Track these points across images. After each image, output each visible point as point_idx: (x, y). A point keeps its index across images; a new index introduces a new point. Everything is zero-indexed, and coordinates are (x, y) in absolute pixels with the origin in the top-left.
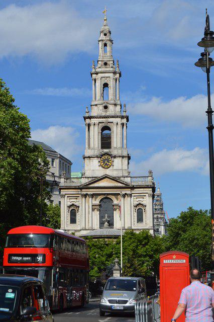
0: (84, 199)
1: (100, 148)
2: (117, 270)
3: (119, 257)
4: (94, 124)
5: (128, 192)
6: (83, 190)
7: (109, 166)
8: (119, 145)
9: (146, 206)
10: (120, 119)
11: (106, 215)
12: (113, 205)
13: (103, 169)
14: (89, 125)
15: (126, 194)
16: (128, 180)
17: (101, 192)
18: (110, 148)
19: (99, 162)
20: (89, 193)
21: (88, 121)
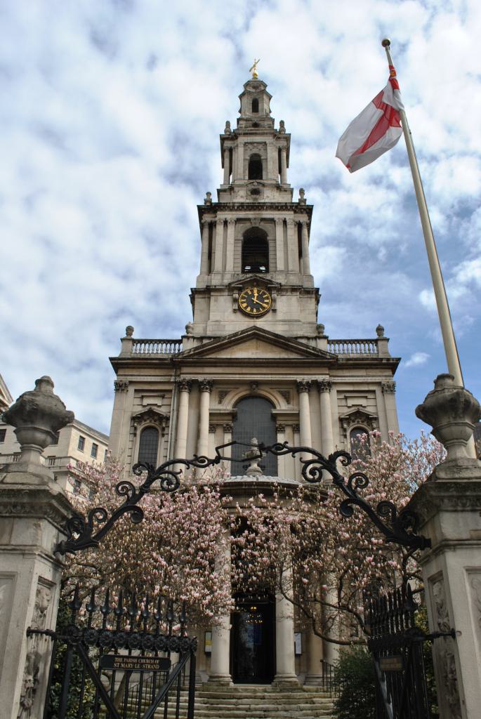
0: (185, 397)
4: (226, 223)
5: (320, 378)
6: (185, 370)
9: (376, 419)
12: (274, 417)
13: (247, 319)
14: (212, 226)
16: (322, 345)
17: (237, 377)
19: (235, 300)
20: (200, 378)
21: (208, 218)
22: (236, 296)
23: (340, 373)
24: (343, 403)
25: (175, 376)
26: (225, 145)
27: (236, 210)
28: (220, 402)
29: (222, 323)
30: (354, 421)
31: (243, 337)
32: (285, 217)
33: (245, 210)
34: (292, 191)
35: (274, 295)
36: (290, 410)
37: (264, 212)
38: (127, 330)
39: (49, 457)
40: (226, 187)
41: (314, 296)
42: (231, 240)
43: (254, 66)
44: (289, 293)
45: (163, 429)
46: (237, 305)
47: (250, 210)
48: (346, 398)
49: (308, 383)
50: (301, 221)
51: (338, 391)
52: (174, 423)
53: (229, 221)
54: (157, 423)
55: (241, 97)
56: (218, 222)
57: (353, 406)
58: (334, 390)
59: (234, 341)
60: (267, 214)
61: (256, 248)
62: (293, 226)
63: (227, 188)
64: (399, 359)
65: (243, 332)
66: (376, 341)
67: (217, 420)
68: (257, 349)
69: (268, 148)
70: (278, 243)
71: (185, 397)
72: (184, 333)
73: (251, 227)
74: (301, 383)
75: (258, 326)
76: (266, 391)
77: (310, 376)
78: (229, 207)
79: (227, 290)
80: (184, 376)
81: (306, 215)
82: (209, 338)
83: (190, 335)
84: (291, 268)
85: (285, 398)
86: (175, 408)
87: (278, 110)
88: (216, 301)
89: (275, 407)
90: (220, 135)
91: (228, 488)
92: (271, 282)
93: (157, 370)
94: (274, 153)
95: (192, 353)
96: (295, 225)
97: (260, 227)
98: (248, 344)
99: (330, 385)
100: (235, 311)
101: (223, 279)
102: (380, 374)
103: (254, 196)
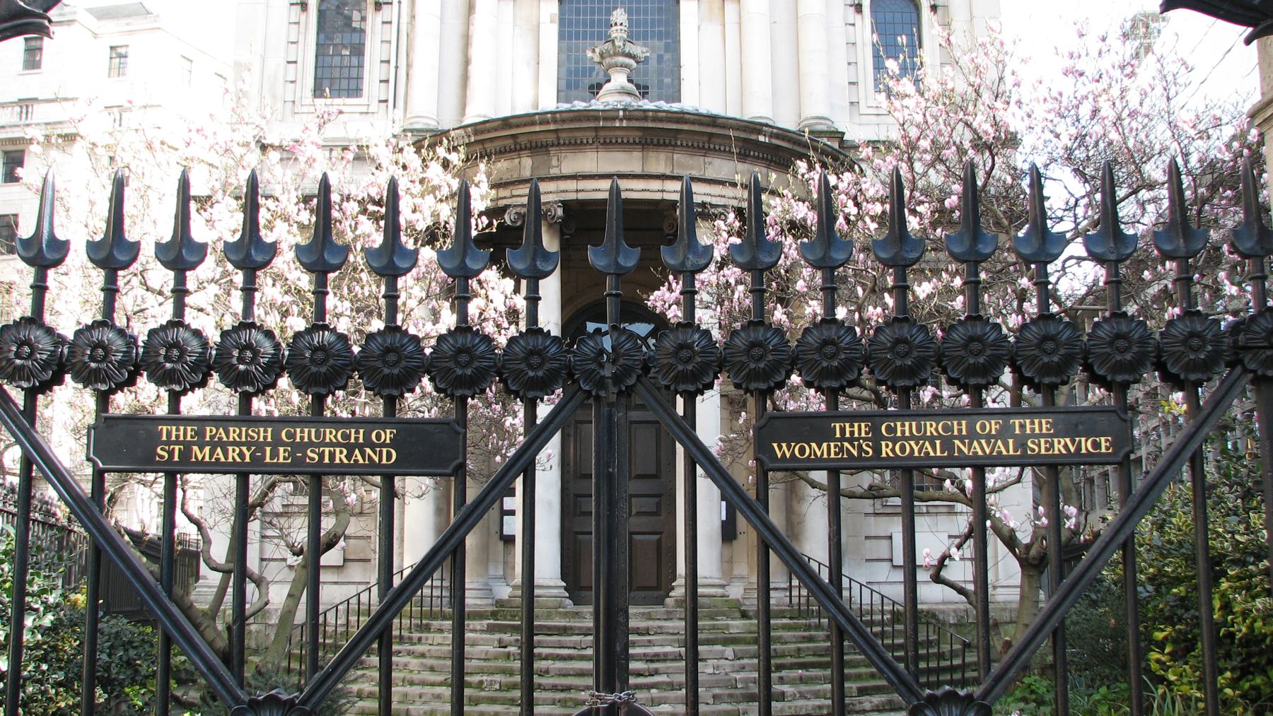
11: (619, 16)
91: (552, 127)
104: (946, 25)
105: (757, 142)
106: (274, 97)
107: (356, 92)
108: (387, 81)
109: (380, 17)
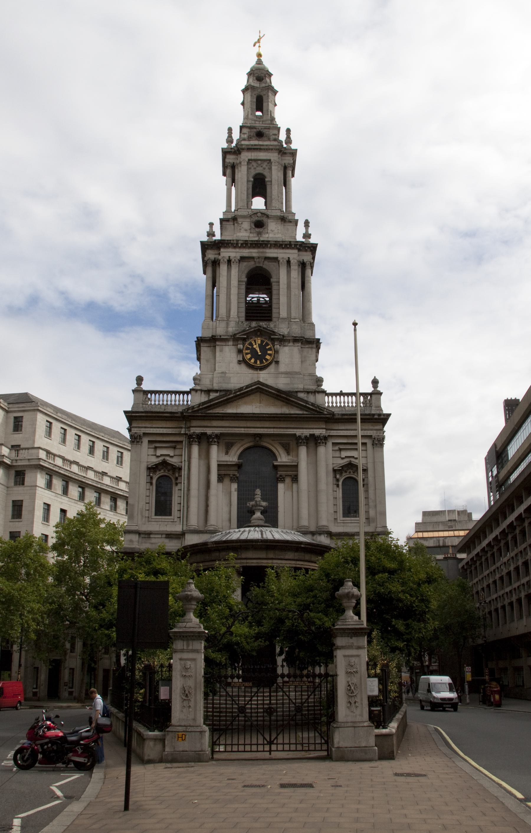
0: (195, 449)
1: (243, 314)
2: (356, 632)
3: (357, 585)
4: (229, 261)
5: (317, 432)
6: (194, 423)
7: (265, 363)
8: (296, 313)
10: (296, 251)
11: (258, 492)
12: (276, 467)
13: (251, 371)
14: (215, 264)
15: (312, 435)
17: (242, 431)
18: (271, 320)
19: (240, 351)
20: (209, 431)
21: (211, 255)
22: (241, 346)
23: (336, 426)
24: (337, 454)
25: (185, 428)
26: (227, 160)
27: (240, 247)
28: (227, 453)
29: (227, 375)
30: (346, 472)
31: (247, 392)
32: (288, 256)
33: (249, 248)
34: (296, 222)
35: (277, 347)
36: (289, 462)
37: (268, 250)
38: (137, 380)
39: (13, 446)
40: (229, 216)
41: (314, 346)
42: (234, 282)
43: (259, 41)
44: (291, 344)
45: (177, 479)
46: (241, 356)
47: (254, 248)
48: (340, 450)
49: (306, 437)
50: (305, 261)
51: (333, 444)
52: (186, 472)
53: (233, 260)
54: (171, 472)
55: (244, 91)
56: (222, 261)
57: (346, 457)
58: (330, 444)
59: (238, 395)
60: (271, 253)
61: (259, 279)
62: (297, 267)
63: (230, 217)
64: (389, 415)
65: (247, 387)
66: (371, 394)
67: (225, 471)
68: (260, 403)
69: (273, 167)
70: (281, 286)
71: (195, 449)
72: (192, 385)
73: (254, 266)
74: (300, 437)
75: (261, 380)
76: (268, 443)
77: (308, 430)
78: (232, 244)
79: (232, 340)
80: (194, 429)
81: (310, 253)
82: (216, 391)
83: (198, 388)
84: (293, 315)
85: (286, 450)
86: (186, 459)
87: (285, 113)
88: (221, 351)
89: (276, 460)
90: (222, 149)
91: (239, 544)
92: (274, 333)
93: (168, 422)
94: (279, 173)
95: (201, 407)
96: (299, 265)
97: (264, 267)
98: (252, 397)
99: (326, 438)
100: (239, 362)
101: (227, 327)
102: (371, 427)
103: (258, 230)
104: (367, 491)
105: (301, 547)
106: (142, 516)
107: (170, 514)
108: (180, 511)
109: (177, 488)
